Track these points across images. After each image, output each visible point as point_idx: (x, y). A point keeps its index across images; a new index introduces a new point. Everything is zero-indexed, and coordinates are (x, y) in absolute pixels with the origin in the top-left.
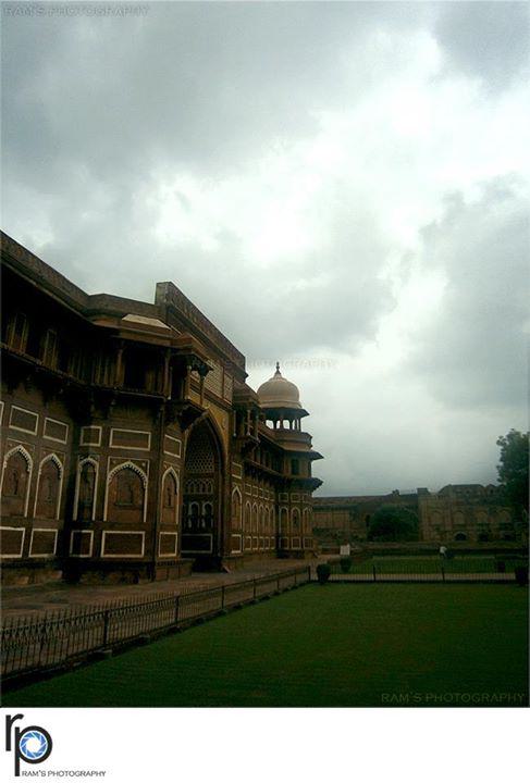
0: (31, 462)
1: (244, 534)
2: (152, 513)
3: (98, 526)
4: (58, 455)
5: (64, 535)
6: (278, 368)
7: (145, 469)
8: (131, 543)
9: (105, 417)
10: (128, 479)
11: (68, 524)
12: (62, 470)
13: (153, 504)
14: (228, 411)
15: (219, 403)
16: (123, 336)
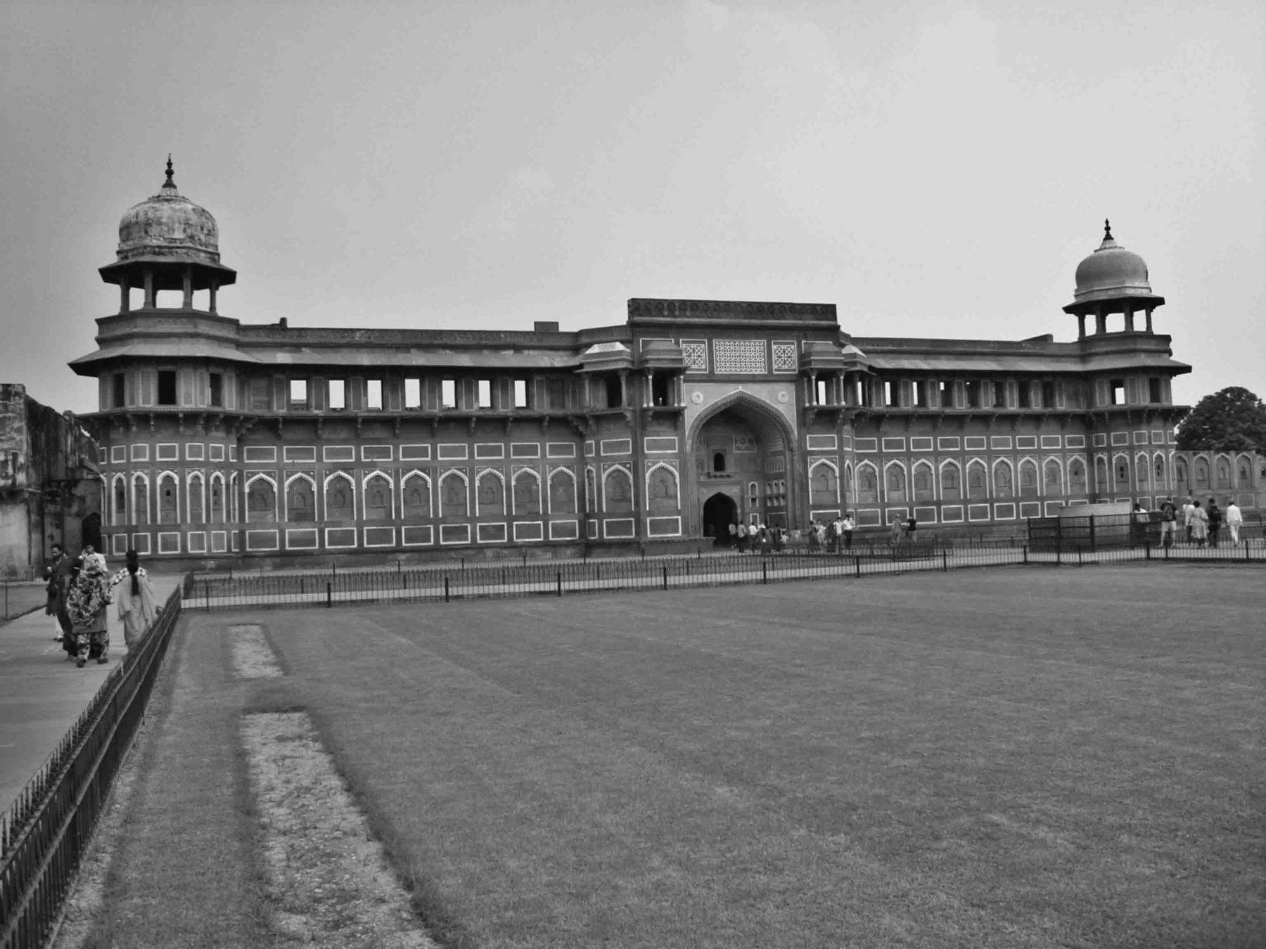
0: (538, 476)
2: (637, 504)
3: (600, 516)
4: (568, 467)
5: (583, 524)
6: (1108, 229)
7: (629, 469)
8: (625, 527)
9: (593, 435)
10: (617, 477)
11: (585, 517)
12: (575, 478)
13: (637, 496)
14: (791, 381)
15: (769, 379)
16: (586, 369)
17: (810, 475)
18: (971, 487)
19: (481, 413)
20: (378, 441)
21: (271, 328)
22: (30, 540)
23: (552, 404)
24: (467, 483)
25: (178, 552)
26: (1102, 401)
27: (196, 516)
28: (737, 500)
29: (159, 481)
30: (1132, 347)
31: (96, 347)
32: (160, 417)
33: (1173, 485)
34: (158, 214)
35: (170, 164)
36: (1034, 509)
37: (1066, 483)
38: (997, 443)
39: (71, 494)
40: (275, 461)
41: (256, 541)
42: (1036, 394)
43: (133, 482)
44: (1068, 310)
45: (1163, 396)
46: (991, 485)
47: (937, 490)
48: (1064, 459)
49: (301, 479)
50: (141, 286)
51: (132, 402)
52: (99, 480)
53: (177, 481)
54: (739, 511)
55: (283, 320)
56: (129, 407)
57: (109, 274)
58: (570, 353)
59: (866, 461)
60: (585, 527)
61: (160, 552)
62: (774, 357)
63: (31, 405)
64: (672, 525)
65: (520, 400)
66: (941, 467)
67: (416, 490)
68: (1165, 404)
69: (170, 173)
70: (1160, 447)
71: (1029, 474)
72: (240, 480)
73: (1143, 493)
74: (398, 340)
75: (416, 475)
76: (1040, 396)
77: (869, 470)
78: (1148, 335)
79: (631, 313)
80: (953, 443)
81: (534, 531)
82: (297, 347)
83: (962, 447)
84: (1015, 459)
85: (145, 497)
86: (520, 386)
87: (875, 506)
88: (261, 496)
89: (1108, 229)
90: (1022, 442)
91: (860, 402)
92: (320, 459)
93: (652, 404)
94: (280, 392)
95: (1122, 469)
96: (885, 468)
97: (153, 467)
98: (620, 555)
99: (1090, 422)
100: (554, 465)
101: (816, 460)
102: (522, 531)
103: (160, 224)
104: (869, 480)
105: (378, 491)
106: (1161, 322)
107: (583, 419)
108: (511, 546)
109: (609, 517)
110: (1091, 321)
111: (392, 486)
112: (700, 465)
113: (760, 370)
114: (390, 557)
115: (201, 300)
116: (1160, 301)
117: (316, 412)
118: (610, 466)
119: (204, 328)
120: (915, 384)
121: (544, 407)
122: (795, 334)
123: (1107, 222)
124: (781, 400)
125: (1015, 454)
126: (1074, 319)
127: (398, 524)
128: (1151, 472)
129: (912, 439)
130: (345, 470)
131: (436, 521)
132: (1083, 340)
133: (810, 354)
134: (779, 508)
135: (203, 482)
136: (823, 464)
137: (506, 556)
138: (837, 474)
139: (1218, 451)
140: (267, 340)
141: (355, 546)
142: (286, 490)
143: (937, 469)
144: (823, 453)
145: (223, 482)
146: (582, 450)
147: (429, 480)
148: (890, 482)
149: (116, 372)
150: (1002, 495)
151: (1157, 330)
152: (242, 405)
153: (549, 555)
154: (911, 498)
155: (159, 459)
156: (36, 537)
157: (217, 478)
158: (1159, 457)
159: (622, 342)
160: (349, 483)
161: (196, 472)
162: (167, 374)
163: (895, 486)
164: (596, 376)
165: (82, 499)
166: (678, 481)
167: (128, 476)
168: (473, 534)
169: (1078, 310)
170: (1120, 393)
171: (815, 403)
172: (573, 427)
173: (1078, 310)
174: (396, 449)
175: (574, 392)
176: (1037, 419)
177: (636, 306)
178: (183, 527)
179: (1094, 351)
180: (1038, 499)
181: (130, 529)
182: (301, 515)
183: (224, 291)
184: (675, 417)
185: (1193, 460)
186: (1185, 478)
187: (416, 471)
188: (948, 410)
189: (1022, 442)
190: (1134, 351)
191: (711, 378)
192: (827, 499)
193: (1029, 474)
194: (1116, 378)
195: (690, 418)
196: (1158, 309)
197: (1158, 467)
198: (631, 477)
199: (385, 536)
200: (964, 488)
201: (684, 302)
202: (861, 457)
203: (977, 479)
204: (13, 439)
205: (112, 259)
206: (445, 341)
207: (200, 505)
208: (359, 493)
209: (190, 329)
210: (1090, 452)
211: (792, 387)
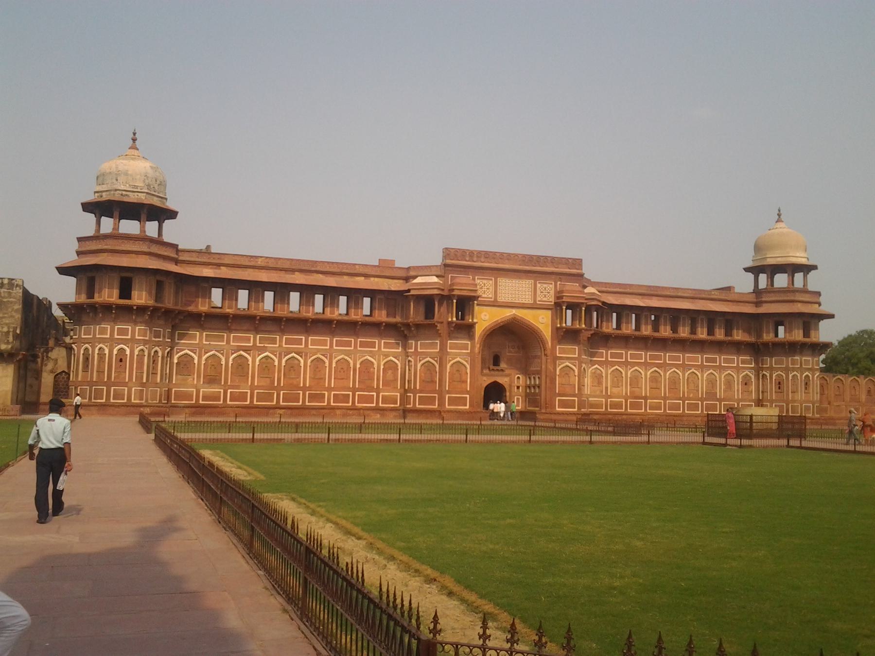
3: (415, 391)
6: (779, 215)
8: (431, 400)
10: (428, 366)
11: (406, 391)
15: (533, 307)
16: (412, 292)
17: (558, 373)
19: (340, 318)
20: (269, 332)
21: (200, 252)
22: (18, 387)
23: (388, 316)
24: (327, 364)
25: (125, 401)
27: (139, 377)
28: (506, 386)
29: (115, 352)
30: (792, 298)
31: (76, 258)
32: (119, 307)
33: (817, 397)
34: (126, 168)
35: (134, 134)
36: (714, 407)
37: (738, 390)
38: (690, 359)
39: (47, 356)
40: (197, 342)
41: (180, 396)
43: (97, 351)
44: (747, 270)
45: (813, 333)
46: (683, 388)
47: (645, 389)
49: (214, 355)
50: (111, 216)
51: (100, 297)
52: (71, 349)
53: (128, 352)
54: (508, 394)
55: (208, 247)
56: (97, 298)
57: (88, 207)
58: (401, 281)
60: (404, 398)
61: (112, 401)
62: (538, 292)
63: (26, 293)
64: (463, 401)
65: (366, 310)
66: (649, 373)
67: (292, 367)
68: (813, 338)
69: (134, 140)
71: (712, 383)
72: (170, 354)
73: (794, 401)
74: (287, 266)
75: (293, 357)
76: (723, 331)
77: (598, 372)
78: (804, 291)
79: (445, 257)
81: (369, 399)
82: (219, 265)
85: (104, 362)
86: (367, 301)
87: (603, 397)
88: (185, 365)
89: (779, 215)
90: (708, 360)
91: (595, 325)
92: (228, 342)
93: (454, 319)
94: (204, 297)
95: (779, 383)
97: (112, 341)
98: (427, 418)
99: (758, 350)
100: (386, 356)
101: (562, 363)
102: (362, 399)
103: (126, 174)
104: (598, 378)
105: (266, 367)
106: (814, 281)
107: (407, 325)
108: (354, 408)
109: (421, 391)
110: (763, 278)
111: (276, 363)
112: (483, 361)
113: (529, 300)
114: (271, 411)
115: (151, 228)
116: (815, 267)
117: (228, 310)
118: (424, 359)
119: (155, 249)
120: (634, 315)
121: (382, 316)
122: (553, 277)
124: (542, 322)
125: (702, 368)
126: (751, 276)
127: (278, 389)
128: (801, 387)
129: (628, 354)
130: (244, 351)
131: (304, 389)
132: (757, 291)
133: (561, 292)
134: (535, 394)
135: (146, 353)
136: (567, 366)
137: (350, 415)
138: (576, 374)
139: (852, 375)
140: (197, 260)
141: (248, 403)
142: (203, 362)
143: (646, 375)
144: (568, 358)
145: (160, 354)
146: (405, 347)
147: (302, 361)
148: (612, 381)
149: (90, 274)
151: (810, 288)
152: (176, 304)
153: (378, 416)
154: (626, 394)
155: (116, 337)
156: (22, 385)
157: (156, 352)
158: (807, 376)
159: (437, 276)
160: (248, 360)
161: (142, 347)
162: (126, 281)
163: (616, 384)
164: (418, 298)
165: (56, 360)
166: (468, 371)
167: (93, 348)
168: (329, 400)
169: (756, 270)
170: (781, 329)
172: (401, 332)
173: (756, 270)
174: (281, 341)
175: (402, 307)
176: (719, 346)
177: (448, 253)
178: (130, 385)
179: (763, 299)
180: (717, 400)
181: (91, 384)
182: (212, 379)
183: (167, 223)
184: (470, 327)
185: (832, 380)
186: (826, 392)
187: (293, 354)
188: (656, 334)
191: (495, 304)
192: (568, 390)
193: (712, 383)
194: (779, 319)
195: (479, 331)
196: (813, 272)
198: (437, 366)
199: (269, 397)
201: (480, 252)
203: (674, 383)
204: (12, 316)
205: (90, 197)
206: (318, 268)
207: (142, 367)
208: (253, 367)
209: (144, 248)
210: (758, 371)
211: (549, 313)
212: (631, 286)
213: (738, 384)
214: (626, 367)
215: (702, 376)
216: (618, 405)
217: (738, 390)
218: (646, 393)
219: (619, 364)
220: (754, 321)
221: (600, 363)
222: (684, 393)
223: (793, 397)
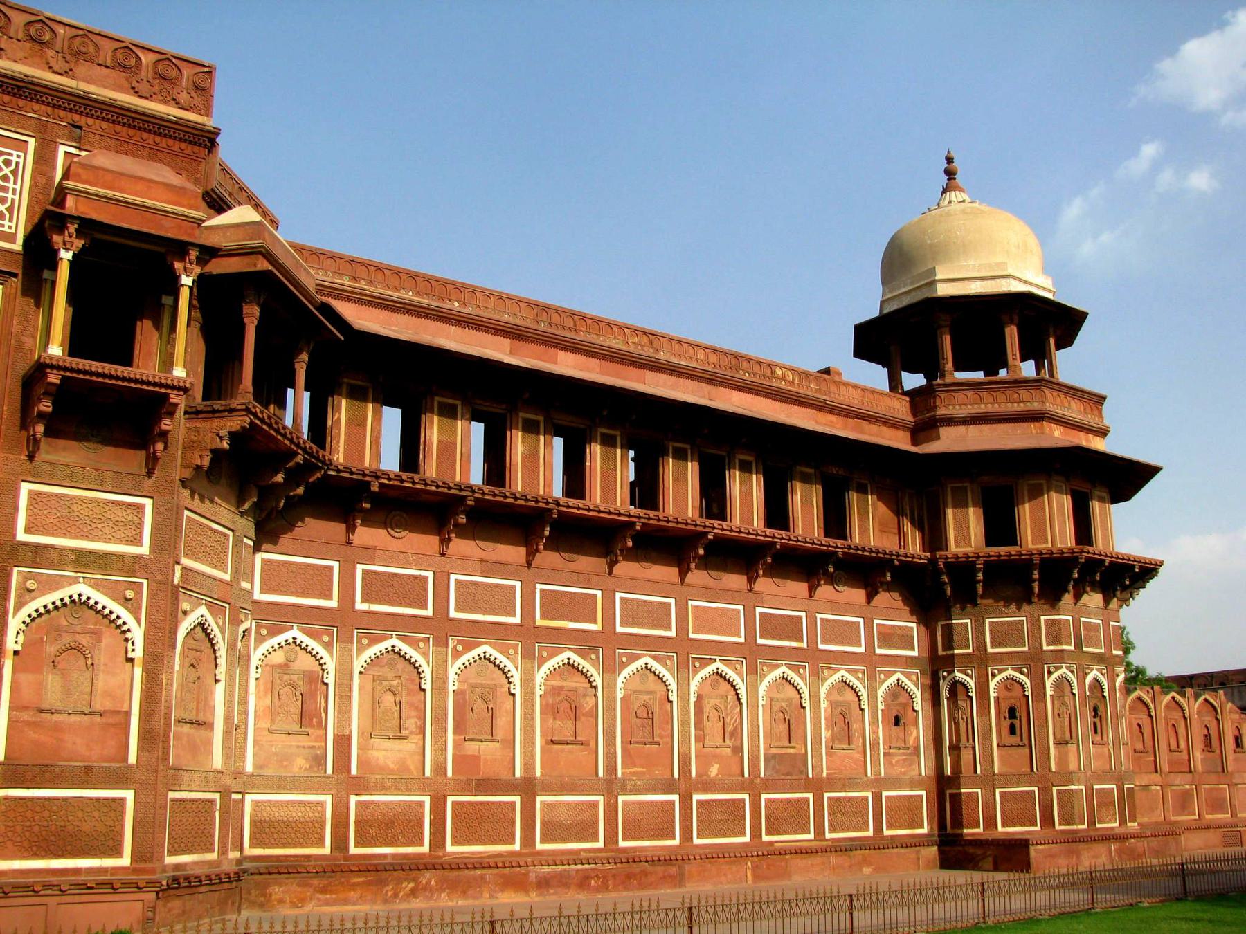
1: (611, 787)
6: (950, 174)
18: (628, 743)
26: (964, 535)
30: (1036, 406)
37: (875, 745)
42: (806, 502)
46: (683, 739)
48: (872, 678)
59: (295, 632)
66: (540, 676)
70: (1099, 659)
73: (1068, 777)
80: (584, 609)
83: (609, 620)
84: (753, 670)
89: (950, 174)
90: (773, 627)
96: (358, 665)
99: (933, 591)
101: (55, 584)
122: (35, 112)
123: (949, 160)
125: (751, 657)
138: (138, 653)
143: (528, 682)
144: (84, 560)
150: (714, 771)
154: (439, 769)
158: (1097, 684)
171: (56, 350)
179: (941, 412)
180: (808, 785)
189: (773, 627)
190: (1038, 417)
192: (81, 746)
194: (997, 483)
197: (1095, 710)
200: (607, 741)
202: (274, 619)
203: (647, 723)
212: (464, 291)
213: (874, 721)
214: (442, 642)
215: (753, 690)
216: (399, 825)
217: (875, 745)
218: (528, 766)
219: (404, 625)
220: (918, 483)
221: (312, 619)
222: (685, 759)
223: (1062, 760)
